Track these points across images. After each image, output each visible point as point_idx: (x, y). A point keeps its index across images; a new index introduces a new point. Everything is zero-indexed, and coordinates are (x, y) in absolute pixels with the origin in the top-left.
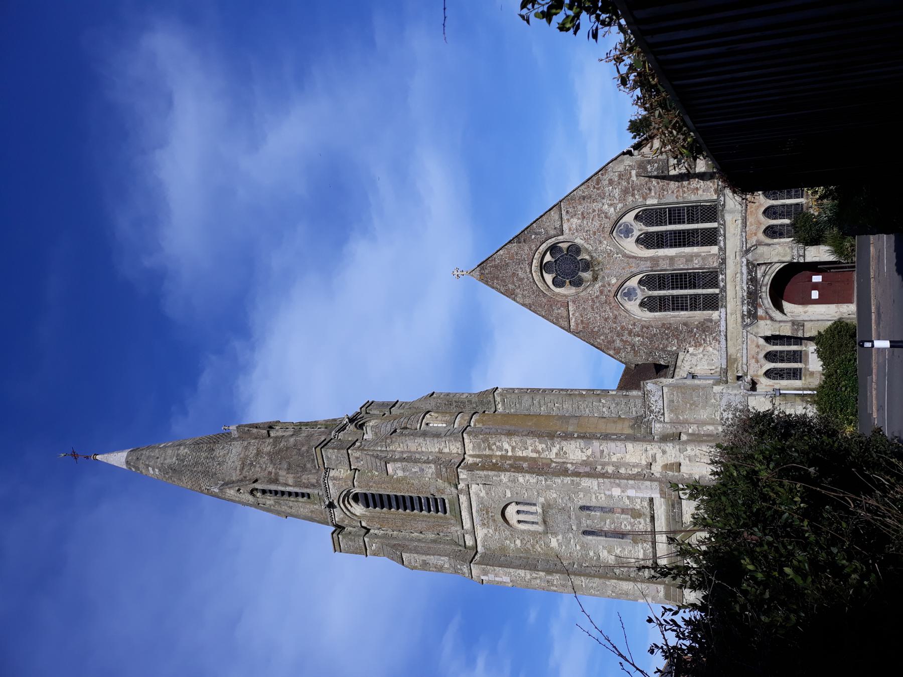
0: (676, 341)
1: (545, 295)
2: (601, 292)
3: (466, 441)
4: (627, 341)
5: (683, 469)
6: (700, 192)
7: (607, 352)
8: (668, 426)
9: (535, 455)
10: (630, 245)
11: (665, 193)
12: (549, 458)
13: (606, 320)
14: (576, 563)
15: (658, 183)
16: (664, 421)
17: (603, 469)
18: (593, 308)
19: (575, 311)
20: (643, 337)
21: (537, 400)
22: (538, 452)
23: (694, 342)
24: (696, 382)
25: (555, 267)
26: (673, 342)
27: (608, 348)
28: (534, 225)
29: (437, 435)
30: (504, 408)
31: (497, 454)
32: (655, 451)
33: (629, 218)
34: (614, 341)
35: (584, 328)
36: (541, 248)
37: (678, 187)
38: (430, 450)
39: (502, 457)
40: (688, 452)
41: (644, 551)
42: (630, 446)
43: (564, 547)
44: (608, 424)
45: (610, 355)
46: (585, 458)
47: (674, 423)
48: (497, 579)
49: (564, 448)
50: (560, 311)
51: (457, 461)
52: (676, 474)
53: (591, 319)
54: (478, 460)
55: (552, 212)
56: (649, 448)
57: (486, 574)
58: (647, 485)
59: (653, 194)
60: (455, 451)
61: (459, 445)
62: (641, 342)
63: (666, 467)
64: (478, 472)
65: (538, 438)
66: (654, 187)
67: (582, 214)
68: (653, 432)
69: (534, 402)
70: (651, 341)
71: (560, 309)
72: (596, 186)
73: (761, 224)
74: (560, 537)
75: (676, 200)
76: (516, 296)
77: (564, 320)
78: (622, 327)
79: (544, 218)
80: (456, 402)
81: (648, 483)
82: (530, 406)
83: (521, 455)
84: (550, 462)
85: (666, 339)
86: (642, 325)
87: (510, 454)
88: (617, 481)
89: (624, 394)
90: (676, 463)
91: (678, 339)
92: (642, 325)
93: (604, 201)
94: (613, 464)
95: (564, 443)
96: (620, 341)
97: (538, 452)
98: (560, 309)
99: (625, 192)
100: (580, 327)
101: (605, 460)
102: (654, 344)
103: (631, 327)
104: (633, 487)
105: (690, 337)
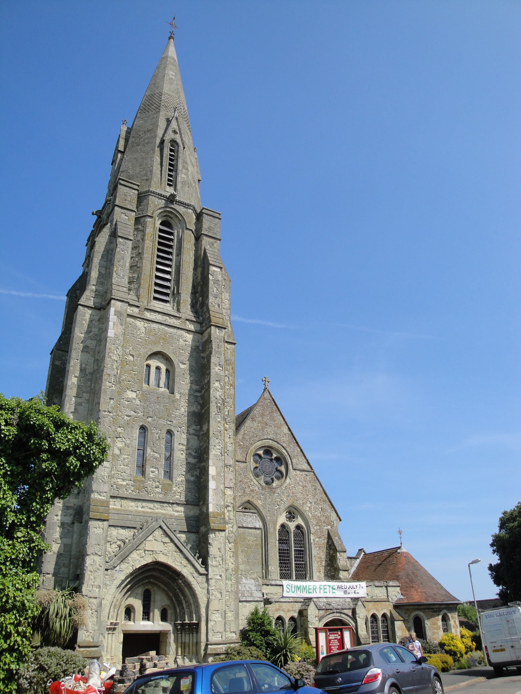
1: (252, 444)
2: (253, 491)
6: (318, 574)
10: (282, 519)
11: (318, 548)
15: (323, 544)
18: (241, 481)
25: (267, 458)
28: (299, 449)
33: (299, 521)
36: (284, 451)
37: (321, 558)
40: (228, 544)
43: (126, 403)
55: (306, 464)
56: (230, 508)
59: (317, 539)
66: (321, 541)
67: (306, 486)
72: (322, 499)
73: (368, 612)
74: (138, 402)
75: (313, 556)
79: (303, 458)
93: (313, 503)
99: (318, 519)
104: (217, 487)
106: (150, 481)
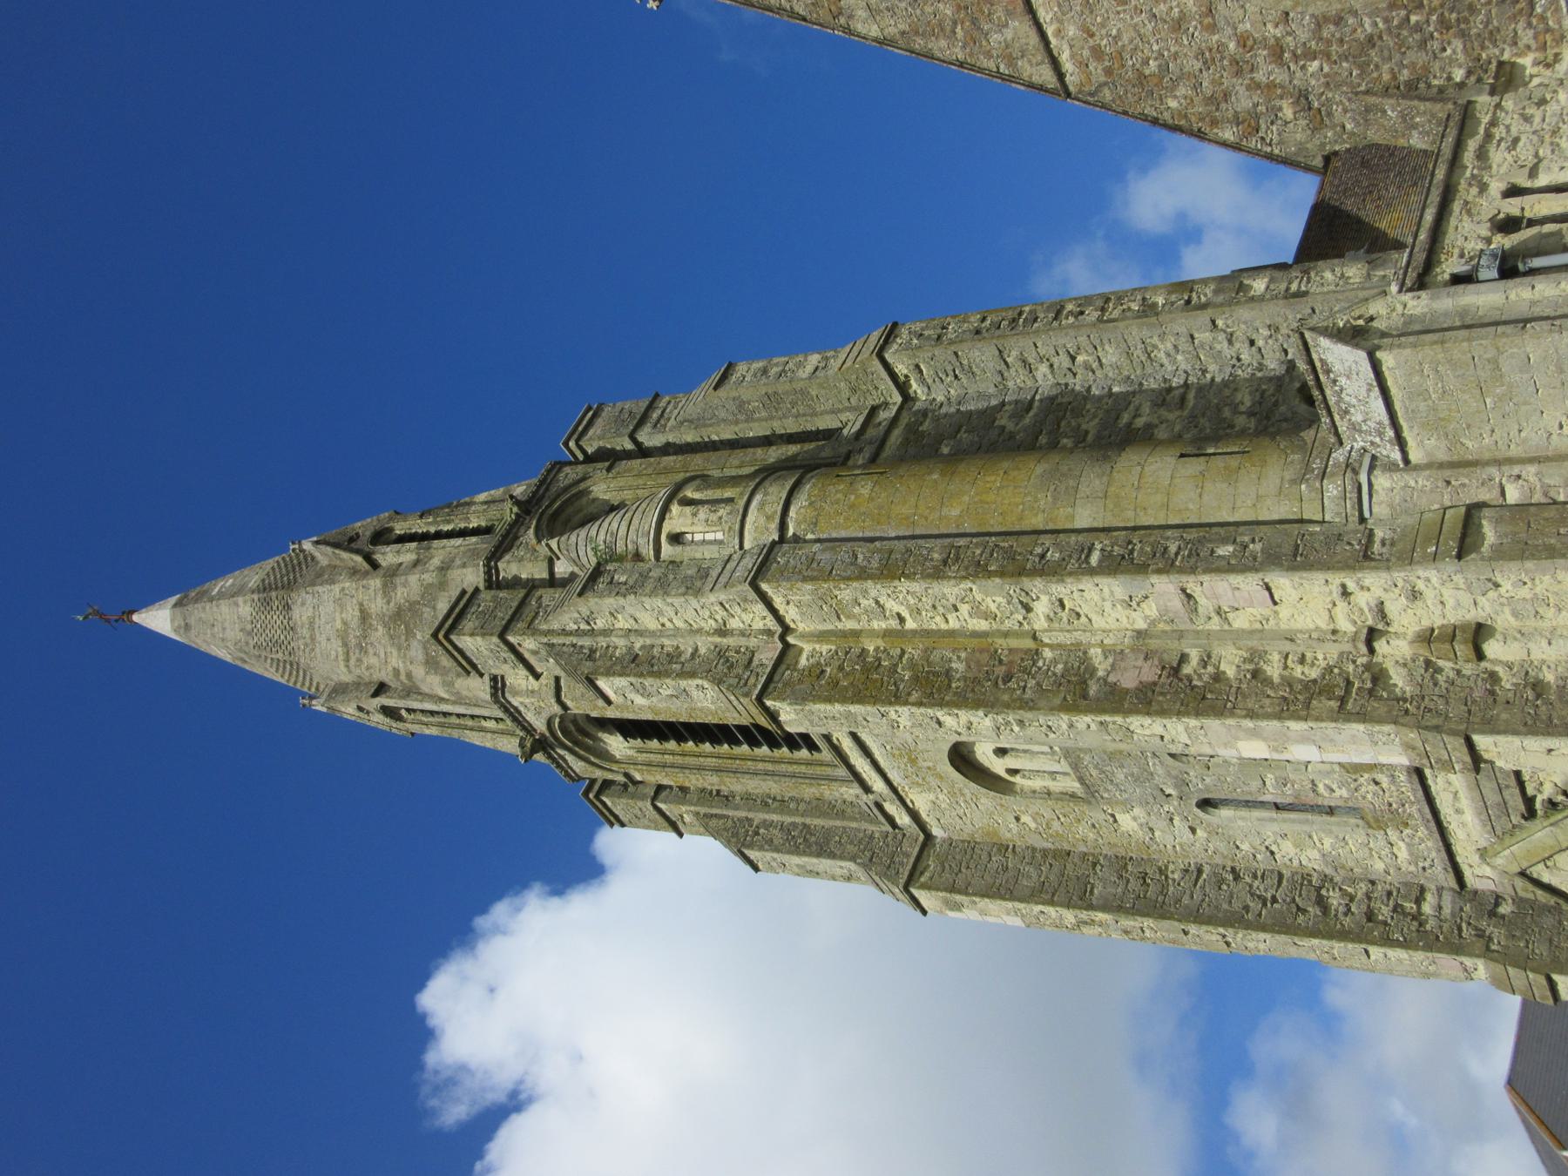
0: (1458, 44)
3: (778, 602)
4: (1271, 86)
5: (1492, 648)
7: (1211, 136)
8: (1422, 481)
9: (982, 625)
12: (1027, 632)
13: (1178, 25)
14: (1207, 869)
16: (1406, 461)
17: (1204, 663)
19: (1060, 22)
20: (1328, 56)
21: (1014, 353)
22: (988, 615)
23: (1530, 33)
24: (1513, 296)
26: (1449, 51)
27: (1214, 123)
29: (696, 580)
30: (926, 390)
31: (876, 627)
32: (1378, 592)
34: (1226, 96)
35: (1108, 72)
38: (695, 626)
39: (887, 634)
41: (1408, 845)
42: (1283, 583)
44: (1209, 486)
45: (1224, 144)
46: (1141, 625)
47: (1441, 466)
48: (990, 919)
49: (1066, 602)
50: (1009, 34)
51: (767, 655)
52: (1468, 669)
53: (1125, 38)
54: (825, 648)
57: (958, 907)
58: (1355, 732)
60: (758, 625)
61: (760, 608)
62: (1326, 76)
63: (1427, 637)
64: (818, 706)
65: (974, 583)
68: (1367, 514)
69: (1008, 360)
70: (1363, 67)
71: (1006, 25)
76: (851, 17)
77: (1034, 61)
78: (1243, 41)
80: (787, 393)
81: (1358, 728)
82: (1000, 372)
83: (943, 626)
84: (1028, 644)
85: (1420, 47)
86: (1312, 16)
87: (910, 624)
88: (1248, 723)
89: (1294, 287)
90: (1464, 627)
91: (1463, 35)
92: (1312, 16)
94: (1237, 636)
95: (1059, 589)
96: (1248, 88)
97: (988, 615)
98: (1006, 25)
100: (1096, 69)
101: (1207, 628)
102: (1375, 75)
103: (1278, 32)
105: (1514, 18)
106: (1364, 798)
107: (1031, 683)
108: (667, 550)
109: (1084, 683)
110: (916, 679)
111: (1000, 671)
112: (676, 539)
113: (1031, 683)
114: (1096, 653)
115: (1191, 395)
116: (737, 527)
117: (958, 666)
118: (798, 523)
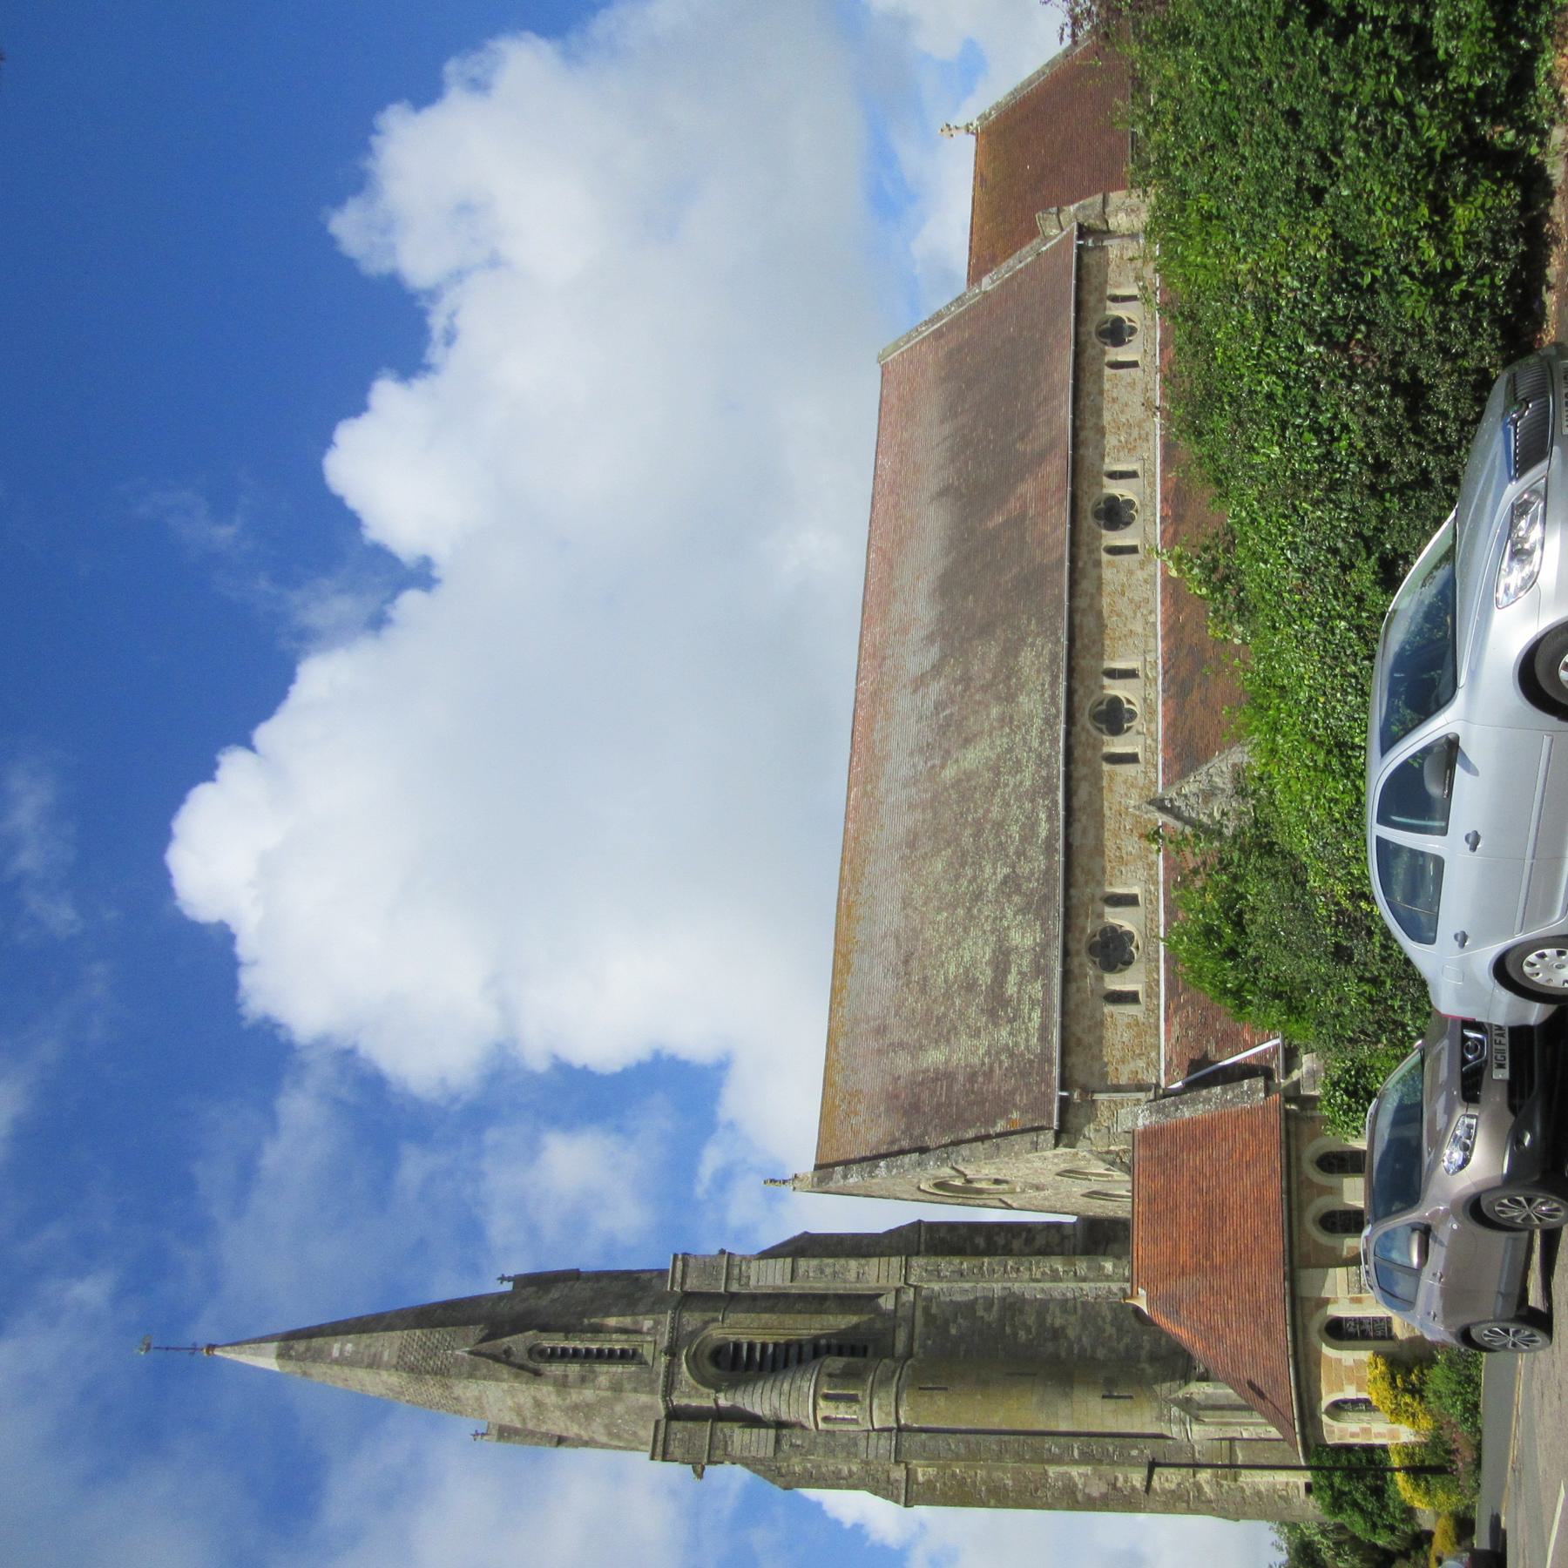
107: (1049, 1494)
108: (821, 1425)
109: (1074, 1493)
110: (989, 1491)
111: (1032, 1486)
112: (826, 1419)
113: (1049, 1494)
114: (1077, 1479)
115: (1079, 1305)
116: (868, 1418)
117: (1009, 1483)
118: (906, 1419)
